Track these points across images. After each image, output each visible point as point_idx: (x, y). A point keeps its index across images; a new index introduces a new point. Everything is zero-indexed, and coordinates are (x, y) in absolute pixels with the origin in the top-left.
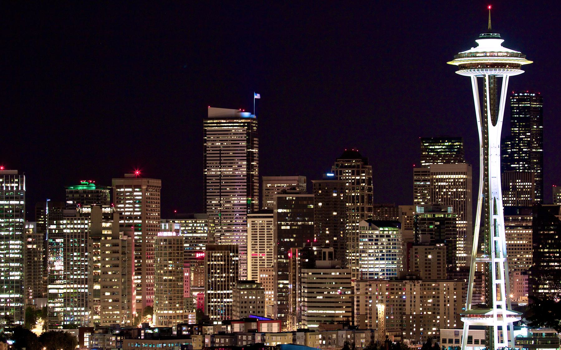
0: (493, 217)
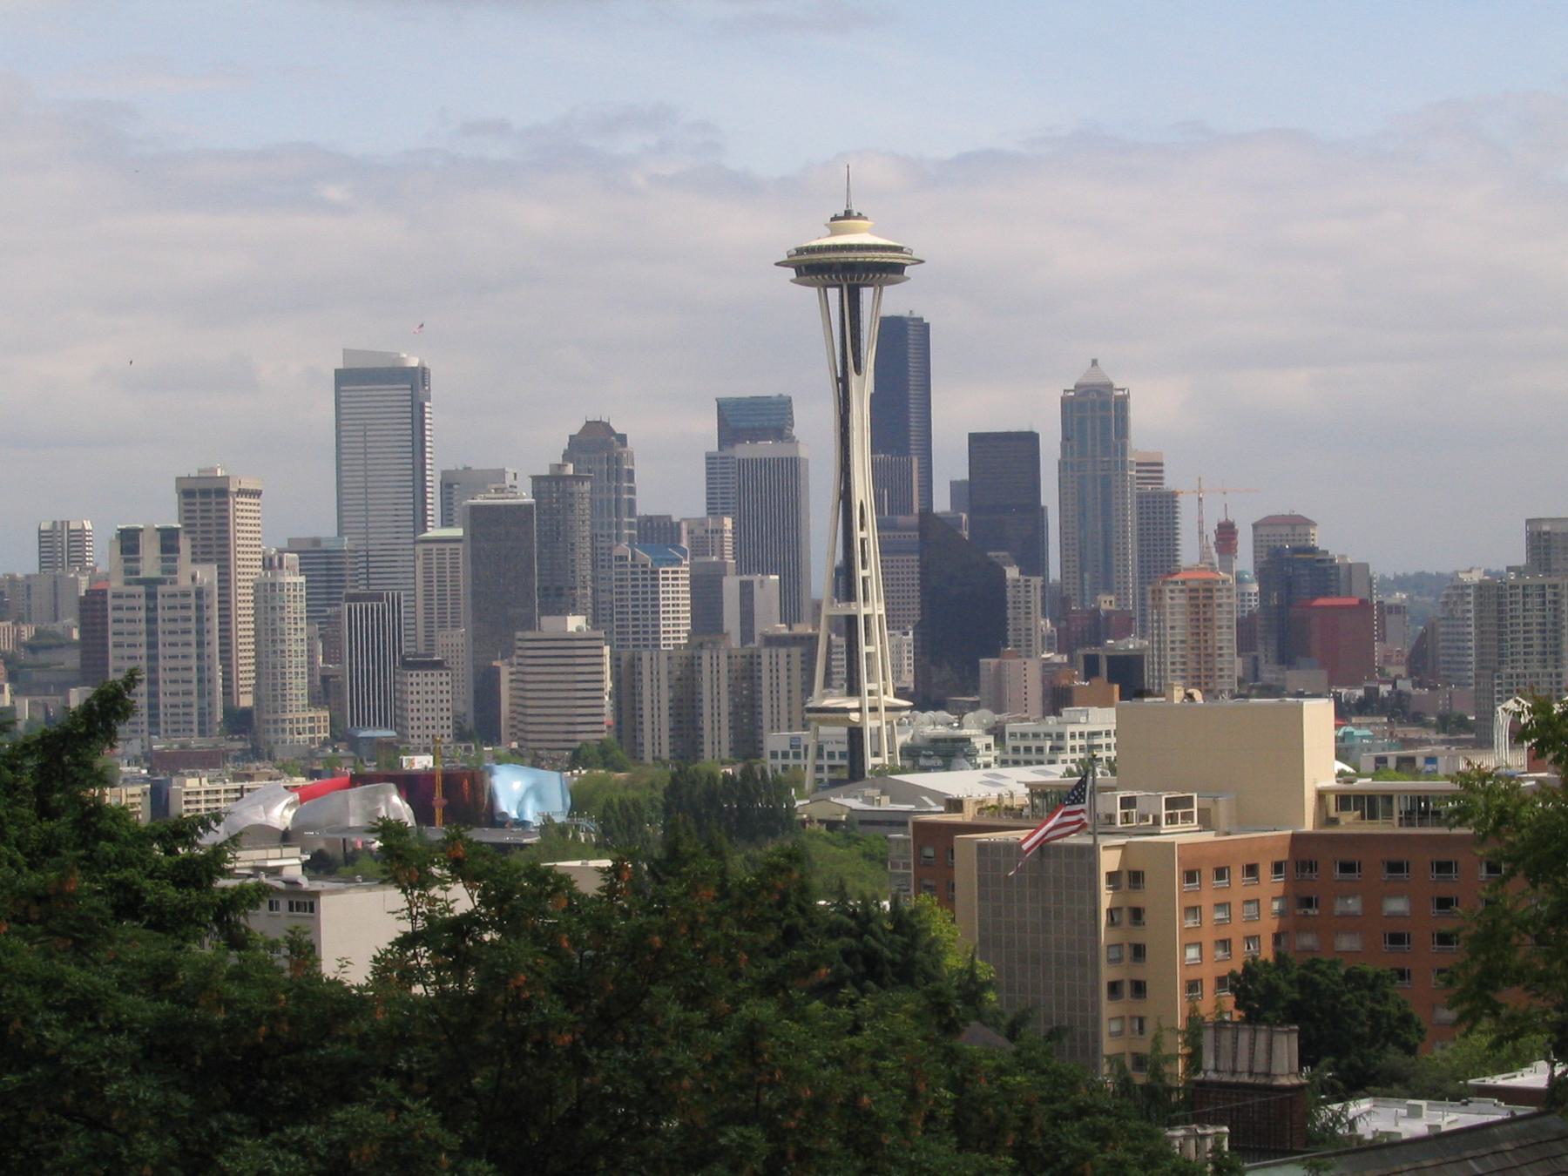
0: (859, 535)
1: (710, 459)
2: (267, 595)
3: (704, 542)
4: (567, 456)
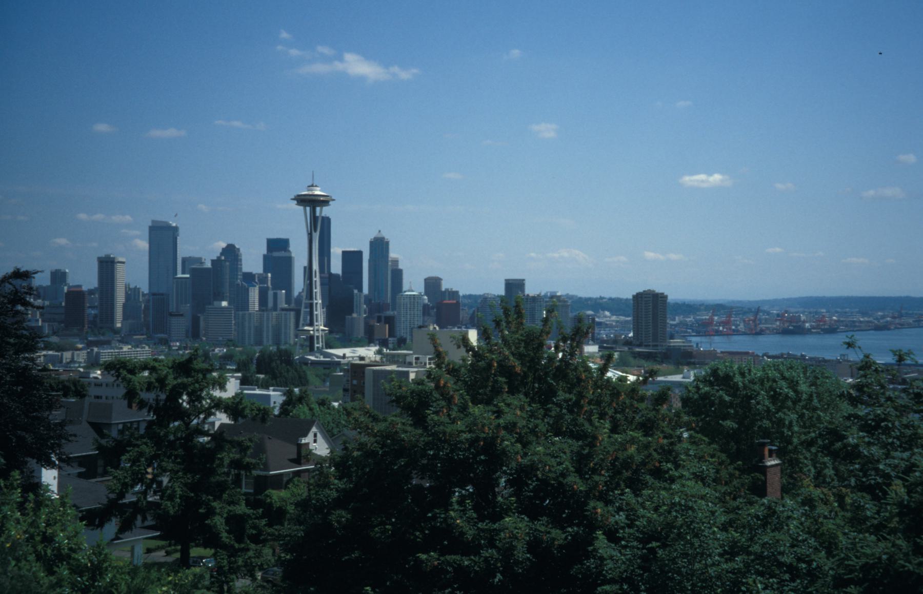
1: (265, 256)
3: (263, 279)
4: (222, 254)
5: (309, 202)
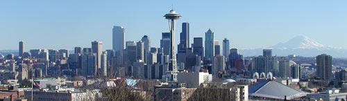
2: (102, 57)
5: (171, 17)
